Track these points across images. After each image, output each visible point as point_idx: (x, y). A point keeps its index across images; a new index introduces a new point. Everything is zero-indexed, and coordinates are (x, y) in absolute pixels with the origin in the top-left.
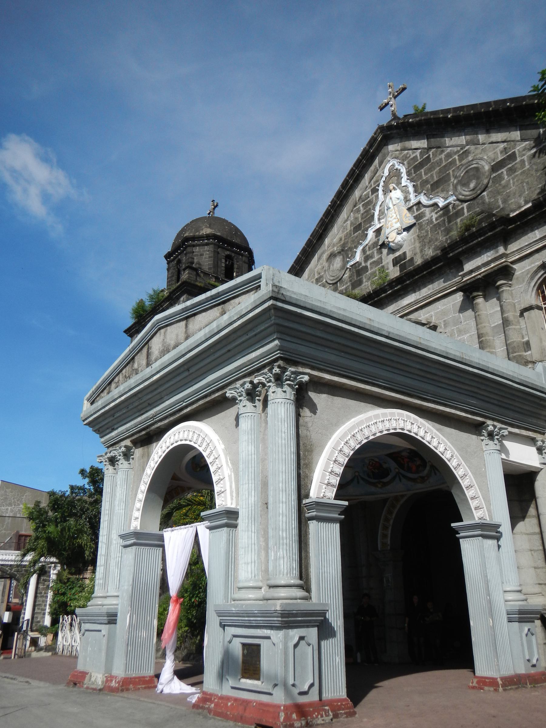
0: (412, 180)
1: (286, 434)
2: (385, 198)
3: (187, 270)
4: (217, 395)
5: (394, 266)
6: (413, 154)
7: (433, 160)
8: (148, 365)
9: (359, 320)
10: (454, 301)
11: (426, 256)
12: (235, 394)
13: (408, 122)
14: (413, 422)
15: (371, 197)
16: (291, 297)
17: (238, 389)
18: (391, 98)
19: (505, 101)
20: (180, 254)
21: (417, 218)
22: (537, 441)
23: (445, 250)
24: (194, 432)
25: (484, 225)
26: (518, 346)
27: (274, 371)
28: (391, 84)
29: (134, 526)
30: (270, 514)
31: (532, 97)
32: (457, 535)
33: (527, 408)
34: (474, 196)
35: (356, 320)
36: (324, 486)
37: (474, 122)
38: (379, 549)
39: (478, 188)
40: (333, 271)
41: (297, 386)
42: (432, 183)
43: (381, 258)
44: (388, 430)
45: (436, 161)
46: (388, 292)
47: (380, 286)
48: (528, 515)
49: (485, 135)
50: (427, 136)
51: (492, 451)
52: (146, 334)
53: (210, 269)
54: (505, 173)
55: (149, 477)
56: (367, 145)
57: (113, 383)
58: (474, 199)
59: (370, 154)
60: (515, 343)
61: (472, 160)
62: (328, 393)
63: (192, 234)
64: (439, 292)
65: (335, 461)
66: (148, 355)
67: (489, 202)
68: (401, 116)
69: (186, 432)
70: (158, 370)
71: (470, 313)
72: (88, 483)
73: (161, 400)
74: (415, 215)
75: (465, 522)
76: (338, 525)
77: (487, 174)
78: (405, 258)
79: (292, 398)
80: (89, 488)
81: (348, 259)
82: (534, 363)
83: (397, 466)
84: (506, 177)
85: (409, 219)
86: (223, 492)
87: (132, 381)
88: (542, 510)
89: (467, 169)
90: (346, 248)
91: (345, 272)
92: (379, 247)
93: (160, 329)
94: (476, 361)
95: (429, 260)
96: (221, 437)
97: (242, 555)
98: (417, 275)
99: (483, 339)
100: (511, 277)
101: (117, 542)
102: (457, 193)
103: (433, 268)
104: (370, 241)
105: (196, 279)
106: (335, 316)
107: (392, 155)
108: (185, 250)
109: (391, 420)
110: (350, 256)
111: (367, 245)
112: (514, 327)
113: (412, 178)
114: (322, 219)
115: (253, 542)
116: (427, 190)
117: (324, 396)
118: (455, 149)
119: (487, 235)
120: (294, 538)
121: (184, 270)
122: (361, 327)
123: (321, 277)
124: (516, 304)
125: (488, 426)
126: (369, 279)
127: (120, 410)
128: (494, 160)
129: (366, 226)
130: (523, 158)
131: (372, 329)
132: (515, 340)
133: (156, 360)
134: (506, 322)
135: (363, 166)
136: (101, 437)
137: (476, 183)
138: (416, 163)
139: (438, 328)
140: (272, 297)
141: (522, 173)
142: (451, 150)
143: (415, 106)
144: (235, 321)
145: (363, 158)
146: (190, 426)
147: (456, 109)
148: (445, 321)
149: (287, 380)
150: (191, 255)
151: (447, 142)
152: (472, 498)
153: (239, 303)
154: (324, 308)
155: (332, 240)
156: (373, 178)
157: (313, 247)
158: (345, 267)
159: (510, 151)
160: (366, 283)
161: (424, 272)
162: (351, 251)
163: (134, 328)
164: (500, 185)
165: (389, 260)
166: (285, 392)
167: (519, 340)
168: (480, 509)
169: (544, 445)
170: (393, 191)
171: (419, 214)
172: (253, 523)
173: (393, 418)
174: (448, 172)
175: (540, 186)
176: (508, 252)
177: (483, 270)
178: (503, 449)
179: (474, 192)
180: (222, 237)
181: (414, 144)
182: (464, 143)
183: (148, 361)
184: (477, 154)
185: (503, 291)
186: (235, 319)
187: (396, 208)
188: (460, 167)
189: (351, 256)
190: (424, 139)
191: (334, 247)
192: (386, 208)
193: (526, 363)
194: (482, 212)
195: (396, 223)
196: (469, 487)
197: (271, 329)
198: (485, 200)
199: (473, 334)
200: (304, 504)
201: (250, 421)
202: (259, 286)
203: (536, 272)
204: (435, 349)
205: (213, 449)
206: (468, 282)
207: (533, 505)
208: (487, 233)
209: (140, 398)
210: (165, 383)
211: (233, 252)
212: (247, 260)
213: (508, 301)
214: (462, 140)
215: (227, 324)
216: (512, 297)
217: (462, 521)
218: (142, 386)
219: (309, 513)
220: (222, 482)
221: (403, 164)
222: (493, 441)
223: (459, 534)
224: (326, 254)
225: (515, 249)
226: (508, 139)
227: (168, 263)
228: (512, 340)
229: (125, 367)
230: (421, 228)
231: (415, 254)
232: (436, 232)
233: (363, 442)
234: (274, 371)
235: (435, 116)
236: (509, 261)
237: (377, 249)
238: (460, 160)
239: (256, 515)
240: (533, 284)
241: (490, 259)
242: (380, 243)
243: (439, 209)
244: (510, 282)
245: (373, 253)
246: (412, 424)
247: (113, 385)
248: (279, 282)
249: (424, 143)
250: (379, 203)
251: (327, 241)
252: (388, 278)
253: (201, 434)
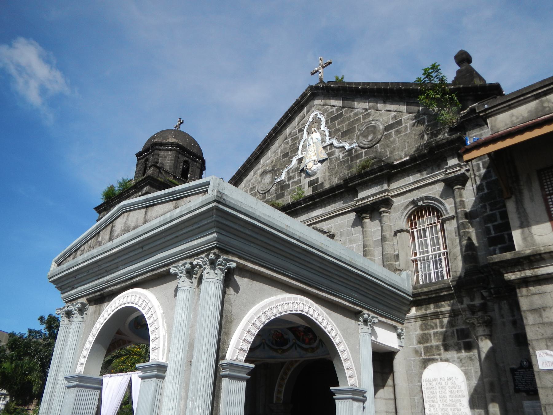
0: (328, 127)
1: (213, 307)
2: (308, 137)
3: (153, 167)
4: (162, 270)
5: (309, 187)
6: (331, 109)
7: (345, 115)
8: (110, 239)
9: (279, 225)
10: (348, 218)
11: (333, 183)
12: (177, 271)
13: (330, 86)
14: (310, 307)
15: (298, 135)
16: (230, 202)
17: (180, 267)
18: (320, 68)
19: (398, 84)
20: (148, 154)
21: (330, 155)
22: (398, 329)
23: (347, 181)
24: (140, 297)
25: (375, 167)
26: (391, 257)
27: (210, 257)
28: (321, 58)
29: (79, 370)
30: (193, 371)
31: (417, 84)
32: (334, 397)
33: (393, 304)
34: (371, 145)
35: (277, 225)
36: (238, 351)
37: (376, 94)
38: (274, 402)
39: (374, 140)
40: (264, 184)
41: (226, 270)
42: (342, 131)
43: (300, 180)
44: (291, 311)
45: (347, 117)
46: (303, 206)
47: (297, 200)
48: (387, 384)
49: (382, 105)
50: (342, 98)
51: (365, 334)
52: (112, 215)
53: (170, 169)
54: (393, 133)
55: (98, 330)
56: (299, 98)
57: (79, 250)
58: (370, 147)
59: (301, 104)
60: (389, 255)
61: (372, 121)
62: (249, 278)
63: (160, 141)
64: (339, 211)
65: (248, 332)
66: (112, 231)
67: (381, 151)
68: (326, 82)
69: (133, 297)
70: (118, 245)
71: (359, 228)
72: (45, 328)
73: (117, 269)
74: (328, 152)
75: (341, 387)
76: (245, 383)
77: (381, 131)
78: (317, 182)
79: (222, 279)
80: (45, 332)
81: (276, 177)
82: (400, 271)
83: (294, 338)
84: (394, 136)
85: (323, 155)
86: (157, 349)
87: (95, 251)
88: (397, 381)
89: (367, 126)
90: (275, 169)
91: (272, 186)
92: (299, 171)
93: (124, 212)
94: (360, 265)
95: (335, 186)
96: (161, 304)
97: (166, 402)
98: (325, 196)
99: (366, 248)
100: (390, 206)
101: (62, 382)
102: (359, 142)
103: (337, 192)
104: (293, 166)
105: (159, 175)
106: (261, 220)
107: (316, 107)
108: (153, 152)
109: (294, 303)
110: (277, 175)
111: (291, 168)
112: (389, 243)
113: (329, 126)
114: (260, 145)
115: (176, 392)
116: (338, 136)
117: (246, 280)
118: (361, 111)
119: (377, 175)
120: (209, 392)
121: (150, 167)
122: (280, 231)
123: (254, 187)
124: (392, 227)
125: (364, 314)
127: (82, 273)
128: (387, 123)
129: (292, 155)
130: (406, 125)
131: (288, 233)
132: (388, 252)
133: (117, 237)
134: (384, 239)
135: (295, 112)
136: (62, 293)
137: (373, 137)
138: (333, 116)
139: (336, 236)
140: (216, 200)
141: (404, 135)
142: (358, 111)
143: (336, 76)
144: (184, 215)
145: (295, 106)
146: (137, 293)
147: (364, 83)
148: (341, 232)
149: (219, 265)
150: (157, 156)
151: (356, 105)
152: (348, 369)
153: (190, 202)
154: (254, 213)
155: (266, 161)
156: (301, 121)
157: (251, 165)
158: (273, 182)
159: (398, 119)
160: (287, 196)
161: (329, 194)
162: (279, 171)
163: (102, 207)
164: (389, 141)
165: (305, 182)
166: (216, 274)
167: (392, 252)
168: (353, 377)
169: (403, 332)
170: (314, 133)
171: (331, 152)
172: (178, 376)
173: (296, 302)
174: (354, 126)
175: (416, 146)
176: (390, 188)
177: (371, 199)
178: (373, 333)
179: (371, 143)
180: (183, 146)
181: (333, 102)
182: (368, 108)
183: (110, 236)
184: (376, 117)
185: (384, 216)
186: (185, 213)
187: (315, 146)
188: (363, 124)
189: (278, 175)
190: (340, 100)
191: (266, 167)
192: (308, 144)
193: (395, 270)
194: (375, 158)
195: (314, 156)
196: (346, 360)
197: (212, 224)
198: (377, 150)
199: (360, 244)
200: (221, 364)
201: (186, 294)
202: (207, 191)
203: (408, 206)
204: (332, 253)
205: (153, 313)
206: (360, 206)
207: (391, 377)
208: (377, 173)
209: (99, 265)
210: (122, 256)
211: (190, 158)
212: (200, 166)
213: (387, 223)
214: (366, 105)
215: (178, 216)
216: (390, 221)
217: (338, 385)
218: (102, 256)
219: (223, 371)
220: (157, 340)
221: (324, 115)
222: (367, 326)
223: (336, 396)
224: (260, 170)
225: (395, 187)
226: (398, 110)
227: (138, 160)
228: (387, 252)
229: (91, 239)
230: (331, 162)
231: (325, 181)
232: (342, 167)
233: (271, 319)
234: (210, 257)
235: (350, 86)
236: (391, 195)
237: (298, 173)
239: (181, 370)
240: (405, 214)
241: (377, 192)
242: (301, 168)
243: (345, 151)
244: (389, 210)
245: (295, 175)
246: (309, 307)
247: (79, 252)
248: (222, 189)
249: (340, 103)
250: (303, 140)
251: (262, 161)
252: (304, 195)
253: (146, 300)
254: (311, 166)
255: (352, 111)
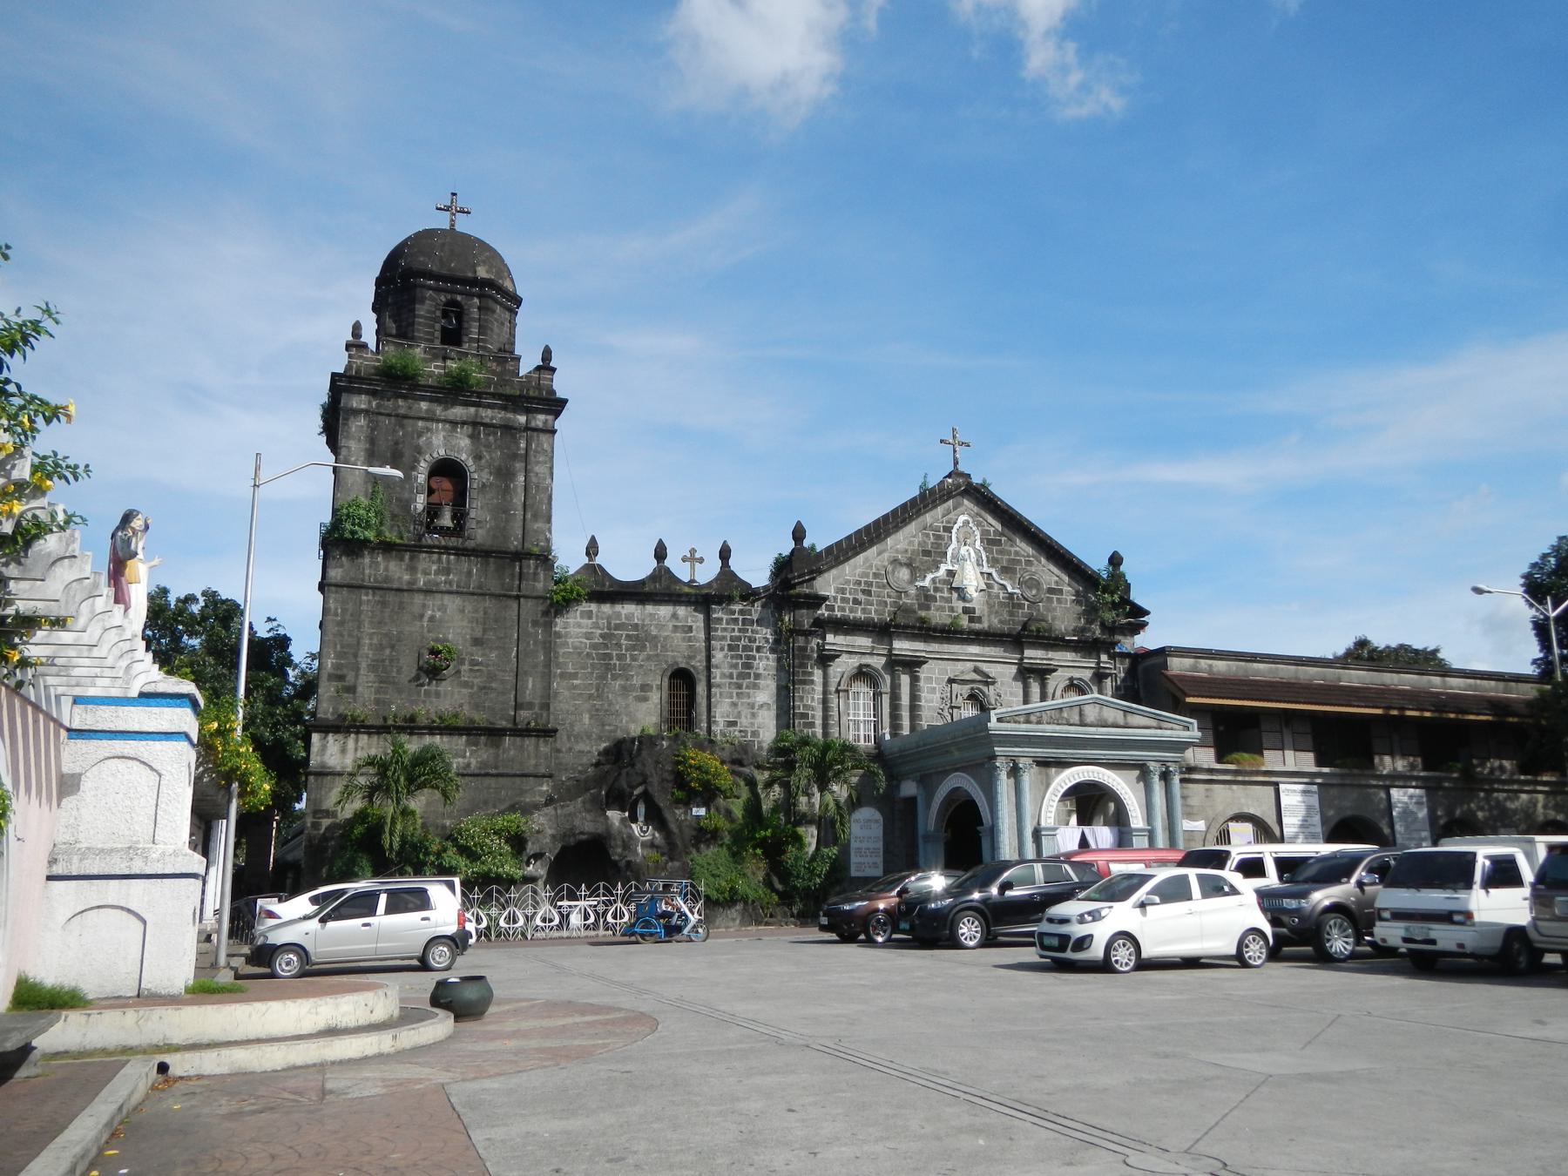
0: (984, 549)
19: (1075, 557)
20: (461, 293)
126: (937, 610)
181: (990, 519)
214: (1030, 550)
230: (989, 595)
238: (1026, 565)
254: (972, 591)
255: (1012, 546)
